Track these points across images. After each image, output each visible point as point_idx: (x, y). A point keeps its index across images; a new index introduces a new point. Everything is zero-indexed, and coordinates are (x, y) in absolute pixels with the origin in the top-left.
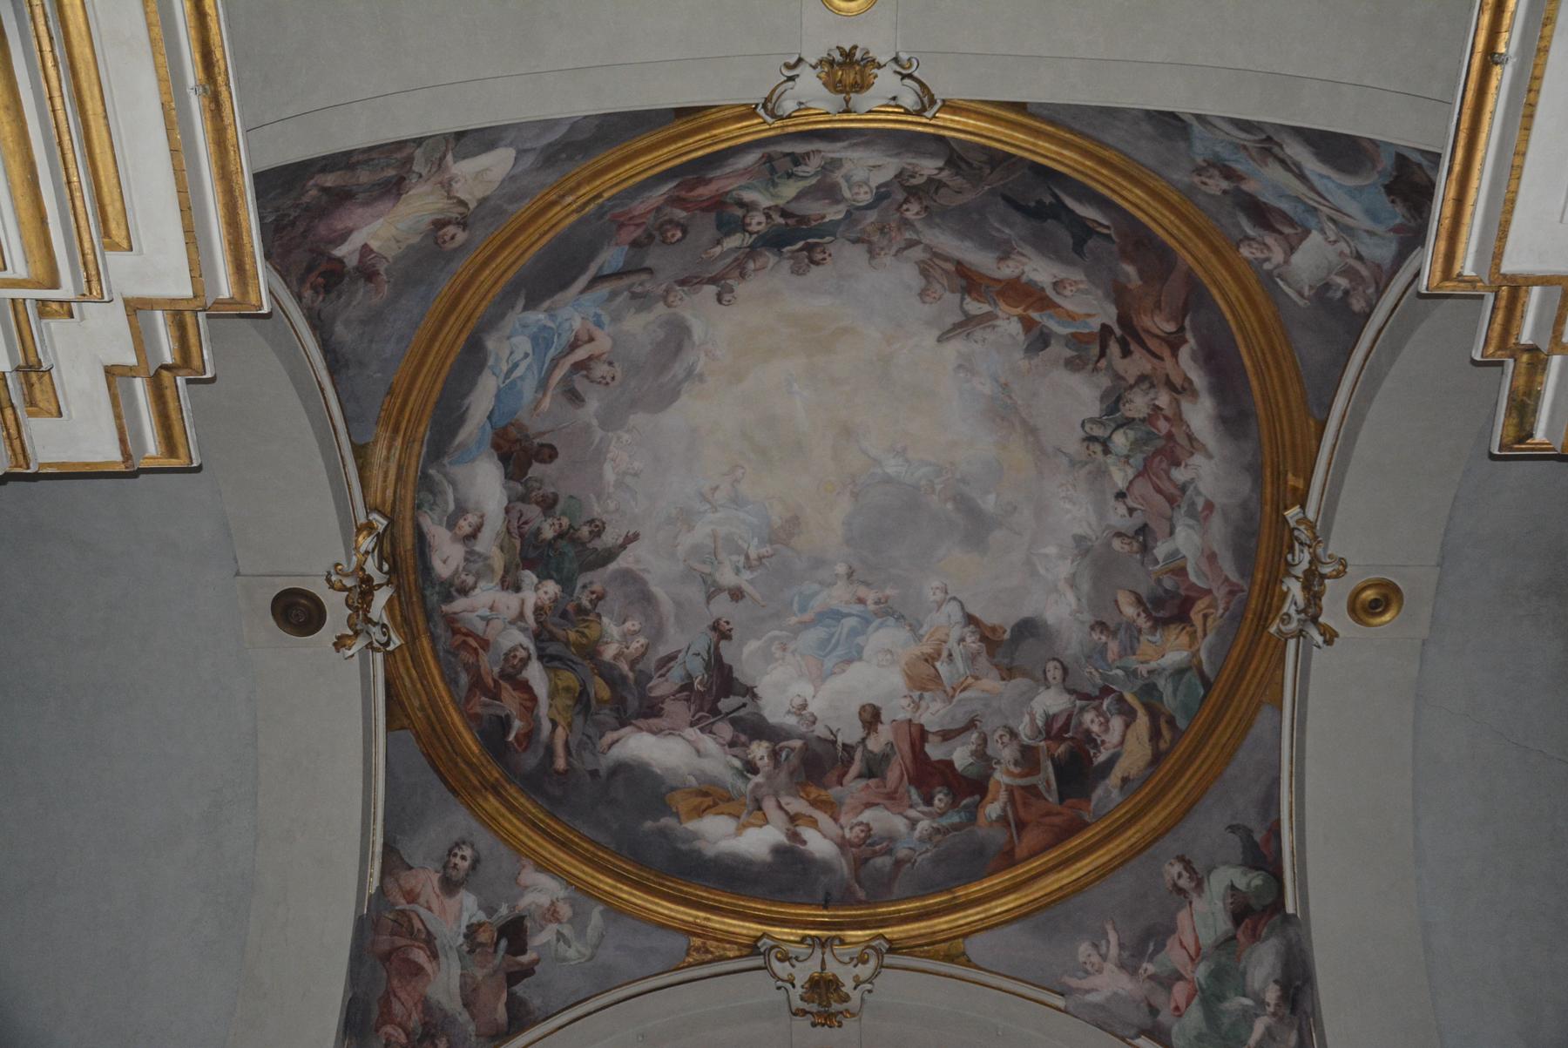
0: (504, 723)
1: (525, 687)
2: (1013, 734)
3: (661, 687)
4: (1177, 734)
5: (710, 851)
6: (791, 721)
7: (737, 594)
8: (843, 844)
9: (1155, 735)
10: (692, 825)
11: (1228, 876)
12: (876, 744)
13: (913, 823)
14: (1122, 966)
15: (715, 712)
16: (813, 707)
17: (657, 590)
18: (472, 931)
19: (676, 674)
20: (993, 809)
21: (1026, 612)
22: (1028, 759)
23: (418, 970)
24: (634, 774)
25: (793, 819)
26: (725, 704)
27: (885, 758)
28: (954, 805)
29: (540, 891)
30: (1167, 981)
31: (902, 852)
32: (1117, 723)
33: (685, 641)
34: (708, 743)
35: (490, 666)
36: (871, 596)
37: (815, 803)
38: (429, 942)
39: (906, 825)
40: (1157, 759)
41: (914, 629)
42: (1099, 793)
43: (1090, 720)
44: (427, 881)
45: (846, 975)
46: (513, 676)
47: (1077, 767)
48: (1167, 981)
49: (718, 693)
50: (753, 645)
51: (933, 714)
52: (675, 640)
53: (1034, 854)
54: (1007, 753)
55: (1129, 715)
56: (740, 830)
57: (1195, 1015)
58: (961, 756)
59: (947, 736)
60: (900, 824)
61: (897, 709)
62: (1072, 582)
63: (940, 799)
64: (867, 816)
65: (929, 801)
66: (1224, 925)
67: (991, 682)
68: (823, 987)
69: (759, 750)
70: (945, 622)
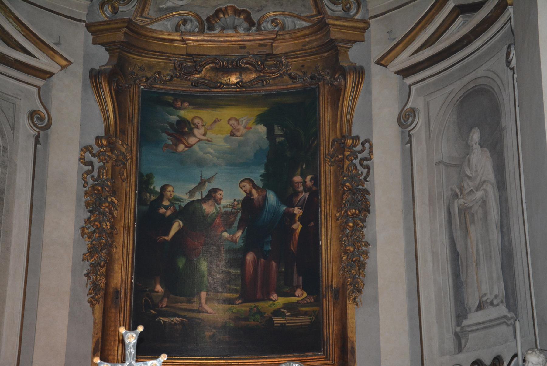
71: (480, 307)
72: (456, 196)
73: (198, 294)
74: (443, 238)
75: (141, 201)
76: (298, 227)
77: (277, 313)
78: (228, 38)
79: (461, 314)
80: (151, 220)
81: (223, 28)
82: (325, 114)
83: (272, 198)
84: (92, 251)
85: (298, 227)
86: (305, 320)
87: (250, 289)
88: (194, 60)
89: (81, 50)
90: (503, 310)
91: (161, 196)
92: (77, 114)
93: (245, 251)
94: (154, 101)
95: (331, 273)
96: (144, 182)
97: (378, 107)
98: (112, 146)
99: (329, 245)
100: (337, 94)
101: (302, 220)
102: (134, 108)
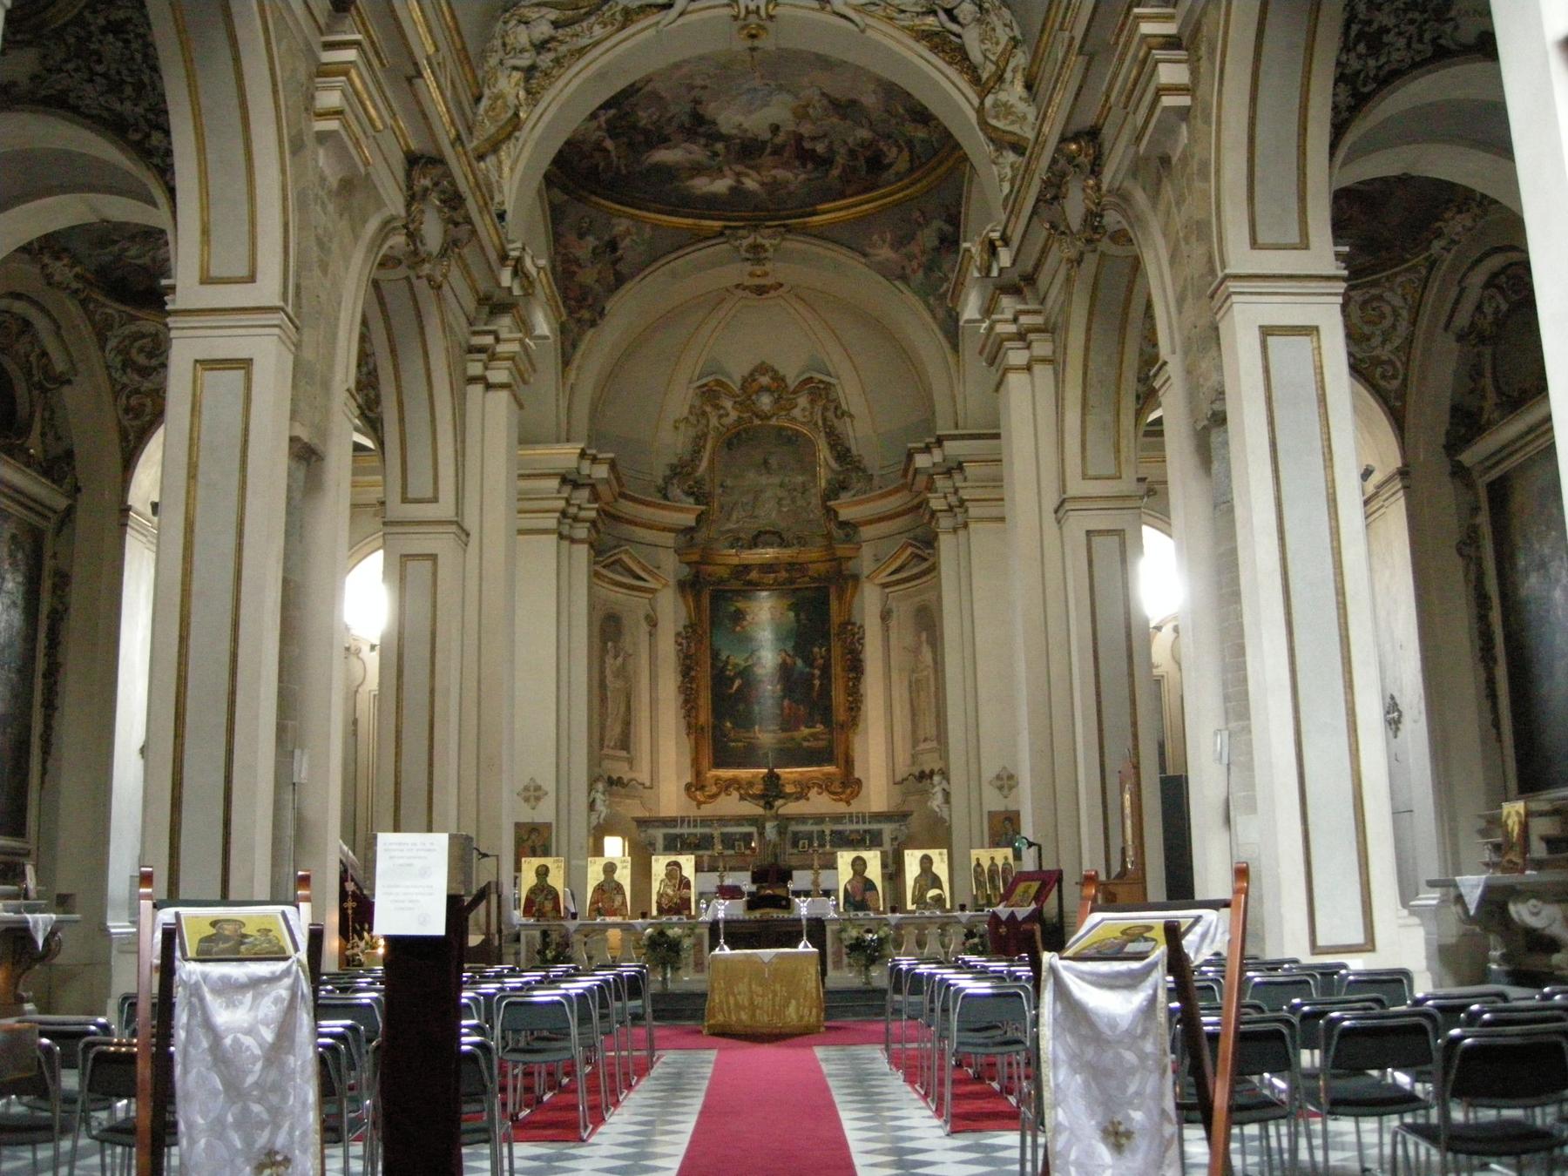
0: (597, 166)
1: (605, 150)
2: (846, 143)
3: (668, 130)
4: (922, 165)
5: (698, 192)
6: (734, 132)
7: (704, 87)
8: (763, 184)
9: (911, 161)
10: (689, 183)
11: (937, 224)
12: (779, 140)
13: (796, 176)
14: (892, 246)
15: (696, 133)
16: (746, 125)
17: (663, 94)
18: (595, 249)
19: (675, 124)
20: (835, 172)
21: (853, 96)
22: (852, 153)
23: (575, 273)
24: (659, 168)
25: (738, 174)
26: (701, 130)
27: (784, 146)
28: (816, 169)
29: (621, 226)
30: (910, 257)
31: (792, 188)
32: (895, 150)
33: (680, 110)
34: (694, 148)
35: (586, 148)
36: (773, 84)
37: (751, 167)
38: (577, 262)
39: (793, 177)
40: (911, 170)
41: (796, 96)
42: (885, 176)
43: (881, 144)
44: (571, 237)
45: (767, 243)
46: (599, 147)
47: (876, 163)
48: (910, 257)
49: (698, 126)
50: (713, 105)
51: (806, 129)
52: (673, 109)
53: (851, 196)
54: (843, 151)
55: (901, 151)
56: (712, 181)
57: (920, 274)
58: (820, 148)
59: (813, 139)
60: (790, 176)
61: (789, 125)
62: (874, 92)
63: (810, 166)
64: (774, 172)
65: (804, 166)
66: (936, 243)
67: (835, 120)
68: (756, 248)
69: (720, 147)
70: (811, 93)
71: (925, 740)
72: (913, 671)
73: (753, 726)
74: (906, 695)
75: (713, 666)
76: (817, 682)
77: (805, 739)
78: (768, 554)
79: (915, 743)
80: (720, 679)
81: (766, 545)
82: (834, 605)
83: (799, 663)
84: (686, 701)
85: (817, 682)
86: (822, 744)
87: (788, 723)
88: (747, 568)
89: (671, 565)
90: (934, 744)
91: (727, 663)
92: (671, 611)
93: (784, 697)
94: (719, 597)
95: (840, 714)
96: (715, 655)
97: (869, 602)
98: (695, 631)
99: (839, 697)
100: (841, 592)
101: (820, 677)
102: (706, 601)
